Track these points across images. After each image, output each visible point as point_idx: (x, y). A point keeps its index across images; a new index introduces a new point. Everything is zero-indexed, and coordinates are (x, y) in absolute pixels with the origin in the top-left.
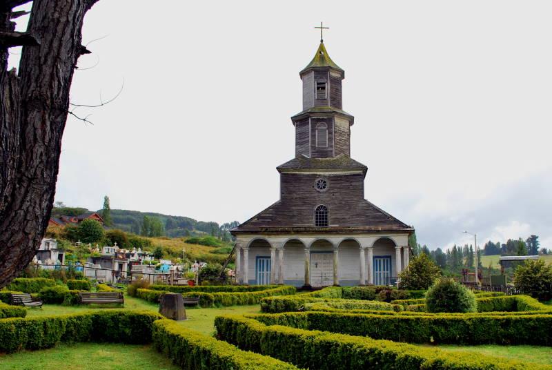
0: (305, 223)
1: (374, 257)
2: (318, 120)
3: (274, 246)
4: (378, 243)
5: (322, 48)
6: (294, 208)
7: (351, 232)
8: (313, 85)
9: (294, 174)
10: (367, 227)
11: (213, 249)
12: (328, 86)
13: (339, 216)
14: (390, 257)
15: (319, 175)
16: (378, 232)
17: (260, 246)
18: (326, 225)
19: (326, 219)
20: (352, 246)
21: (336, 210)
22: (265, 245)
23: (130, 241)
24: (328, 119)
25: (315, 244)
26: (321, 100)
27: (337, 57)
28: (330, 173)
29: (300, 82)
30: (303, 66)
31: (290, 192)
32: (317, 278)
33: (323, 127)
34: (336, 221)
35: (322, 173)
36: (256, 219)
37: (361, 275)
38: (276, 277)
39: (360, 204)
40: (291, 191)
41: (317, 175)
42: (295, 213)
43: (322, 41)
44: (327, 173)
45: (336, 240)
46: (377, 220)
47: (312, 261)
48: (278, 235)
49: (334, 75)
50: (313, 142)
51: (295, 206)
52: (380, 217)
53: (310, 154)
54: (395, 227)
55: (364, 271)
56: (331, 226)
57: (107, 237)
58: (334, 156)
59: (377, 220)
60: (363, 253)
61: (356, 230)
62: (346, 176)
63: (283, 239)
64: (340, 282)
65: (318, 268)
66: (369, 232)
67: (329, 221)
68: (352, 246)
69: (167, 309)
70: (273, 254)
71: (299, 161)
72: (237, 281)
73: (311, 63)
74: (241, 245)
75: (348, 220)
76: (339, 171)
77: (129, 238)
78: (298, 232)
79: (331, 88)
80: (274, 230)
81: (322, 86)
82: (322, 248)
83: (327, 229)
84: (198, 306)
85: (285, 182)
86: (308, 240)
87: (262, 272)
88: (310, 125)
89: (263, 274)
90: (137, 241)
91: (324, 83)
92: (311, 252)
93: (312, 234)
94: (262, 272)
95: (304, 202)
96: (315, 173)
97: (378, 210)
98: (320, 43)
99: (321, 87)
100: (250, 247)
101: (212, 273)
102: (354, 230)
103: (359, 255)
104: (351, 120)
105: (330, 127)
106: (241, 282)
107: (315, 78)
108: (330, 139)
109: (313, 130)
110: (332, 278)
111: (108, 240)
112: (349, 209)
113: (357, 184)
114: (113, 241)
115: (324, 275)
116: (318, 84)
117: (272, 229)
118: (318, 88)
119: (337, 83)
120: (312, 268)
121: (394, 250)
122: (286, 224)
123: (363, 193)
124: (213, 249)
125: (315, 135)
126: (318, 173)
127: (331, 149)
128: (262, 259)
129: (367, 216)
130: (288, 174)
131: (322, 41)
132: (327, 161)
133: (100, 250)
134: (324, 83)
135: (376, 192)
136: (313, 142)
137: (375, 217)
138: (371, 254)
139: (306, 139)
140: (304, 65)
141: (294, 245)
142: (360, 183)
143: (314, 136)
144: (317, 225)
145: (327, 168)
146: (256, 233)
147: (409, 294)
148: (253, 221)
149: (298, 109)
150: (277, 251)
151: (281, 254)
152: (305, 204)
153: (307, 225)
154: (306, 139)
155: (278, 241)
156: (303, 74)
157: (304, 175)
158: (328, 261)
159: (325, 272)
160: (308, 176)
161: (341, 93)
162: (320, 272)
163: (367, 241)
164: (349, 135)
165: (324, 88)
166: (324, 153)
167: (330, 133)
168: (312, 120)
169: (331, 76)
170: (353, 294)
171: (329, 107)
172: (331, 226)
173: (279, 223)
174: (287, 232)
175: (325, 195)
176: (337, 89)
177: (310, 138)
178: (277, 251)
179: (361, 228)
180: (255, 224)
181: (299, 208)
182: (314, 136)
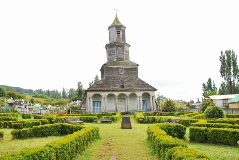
0: (115, 87)
1: (142, 100)
2: (118, 46)
3: (103, 96)
4: (144, 95)
5: (116, 18)
6: (111, 81)
7: (134, 90)
8: (115, 32)
9: (110, 67)
10: (140, 89)
11: (45, 100)
12: (121, 33)
13: (128, 84)
14: (146, 100)
15: (121, 68)
16: (144, 90)
17: (97, 96)
18: (124, 88)
19: (124, 85)
20: (133, 96)
22: (100, 96)
23: (17, 96)
24: (122, 46)
25: (119, 96)
26: (119, 38)
27: (122, 22)
28: (125, 67)
29: (108, 31)
30: (110, 25)
31: (109, 74)
33: (120, 49)
34: (127, 86)
35: (122, 67)
36: (95, 85)
37: (138, 108)
38: (104, 110)
39: (137, 80)
40: (109, 74)
41: (119, 68)
43: (116, 15)
44: (124, 67)
45: (128, 94)
46: (143, 86)
48: (105, 92)
49: (123, 29)
50: (117, 54)
51: (111, 80)
52: (144, 85)
53: (115, 59)
54: (150, 88)
55: (152, 105)
56: (126, 88)
57: (8, 95)
58: (125, 60)
59: (143, 86)
60: (138, 99)
61: (136, 90)
62: (131, 68)
63: (107, 94)
64: (130, 110)
66: (141, 90)
67: (125, 86)
68: (133, 96)
69: (126, 124)
70: (103, 100)
71: (110, 62)
72: (88, 112)
73: (114, 23)
74: (89, 96)
76: (128, 66)
77: (17, 95)
78: (113, 91)
79: (122, 34)
80: (104, 90)
81: (119, 32)
82: (122, 97)
83: (125, 89)
84: (112, 122)
85: (107, 70)
86: (117, 94)
87: (95, 107)
88: (115, 48)
89: (96, 108)
90: (20, 96)
91: (120, 32)
92: (118, 99)
93: (119, 92)
94: (95, 107)
95: (115, 78)
96: (119, 67)
97: (143, 82)
98: (116, 16)
99: (118, 33)
100: (92, 97)
101: (74, 109)
102: (135, 90)
103: (137, 99)
104: (129, 46)
105: (123, 48)
106: (90, 111)
107: (116, 29)
108: (123, 53)
109: (116, 50)
110: (124, 109)
111: (8, 96)
112: (133, 81)
113: (135, 71)
114: (10, 96)
116: (117, 32)
117: (102, 90)
118: (117, 33)
119: (124, 31)
121: (150, 98)
122: (108, 87)
123: (137, 75)
124: (45, 100)
125: (117, 52)
126: (120, 67)
127: (123, 58)
128: (95, 102)
129: (139, 84)
130: (108, 67)
131: (116, 15)
132: (122, 62)
133: (6, 100)
134: (120, 32)
135: (143, 75)
136: (117, 54)
137: (142, 85)
138: (141, 99)
139: (113, 53)
140: (110, 24)
141: (110, 96)
142: (136, 71)
143: (117, 52)
144: (120, 88)
145: (124, 65)
146: (96, 91)
147: (169, 114)
148: (95, 86)
149: (108, 42)
150: (104, 98)
151: (106, 100)
152: (115, 79)
153: (116, 88)
154: (113, 53)
155: (104, 94)
156: (109, 28)
160: (116, 68)
161: (125, 36)
163: (139, 94)
164: (129, 52)
165: (119, 33)
166: (121, 59)
167: (123, 51)
168: (116, 46)
169: (122, 29)
170: (145, 115)
171: (122, 42)
172: (126, 88)
173: (105, 87)
174: (109, 91)
175: (123, 76)
176: (124, 34)
177: (115, 53)
178: (104, 98)
179: (137, 89)
180: (95, 87)
181: (112, 81)
182: (117, 52)
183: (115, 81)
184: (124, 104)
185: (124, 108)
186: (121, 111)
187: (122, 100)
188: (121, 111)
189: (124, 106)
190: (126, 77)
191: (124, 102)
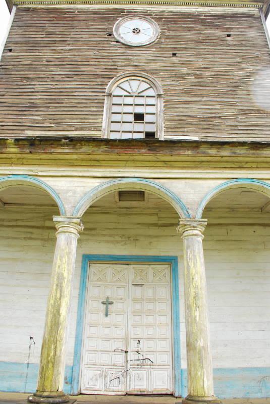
0: (69, 127)
6: (37, 85)
21: (188, 93)
31: (34, 45)
32: (105, 358)
41: (122, 10)
42: (38, 98)
47: (95, 292)
51: (41, 79)
62: (214, 17)
65: (112, 317)
75: (231, 123)
110: (166, 359)
115: (133, 346)
120: (89, 318)
157: (81, 12)
158: (150, 293)
159: (135, 333)
160: (96, 12)
162: (120, 333)
175: (150, 54)
183: (73, 84)
184: (166, 307)
185: (166, 345)
186: (134, 372)
187: (150, 269)
188: (134, 372)
189: (167, 332)
190: (173, 64)
191: (164, 292)
